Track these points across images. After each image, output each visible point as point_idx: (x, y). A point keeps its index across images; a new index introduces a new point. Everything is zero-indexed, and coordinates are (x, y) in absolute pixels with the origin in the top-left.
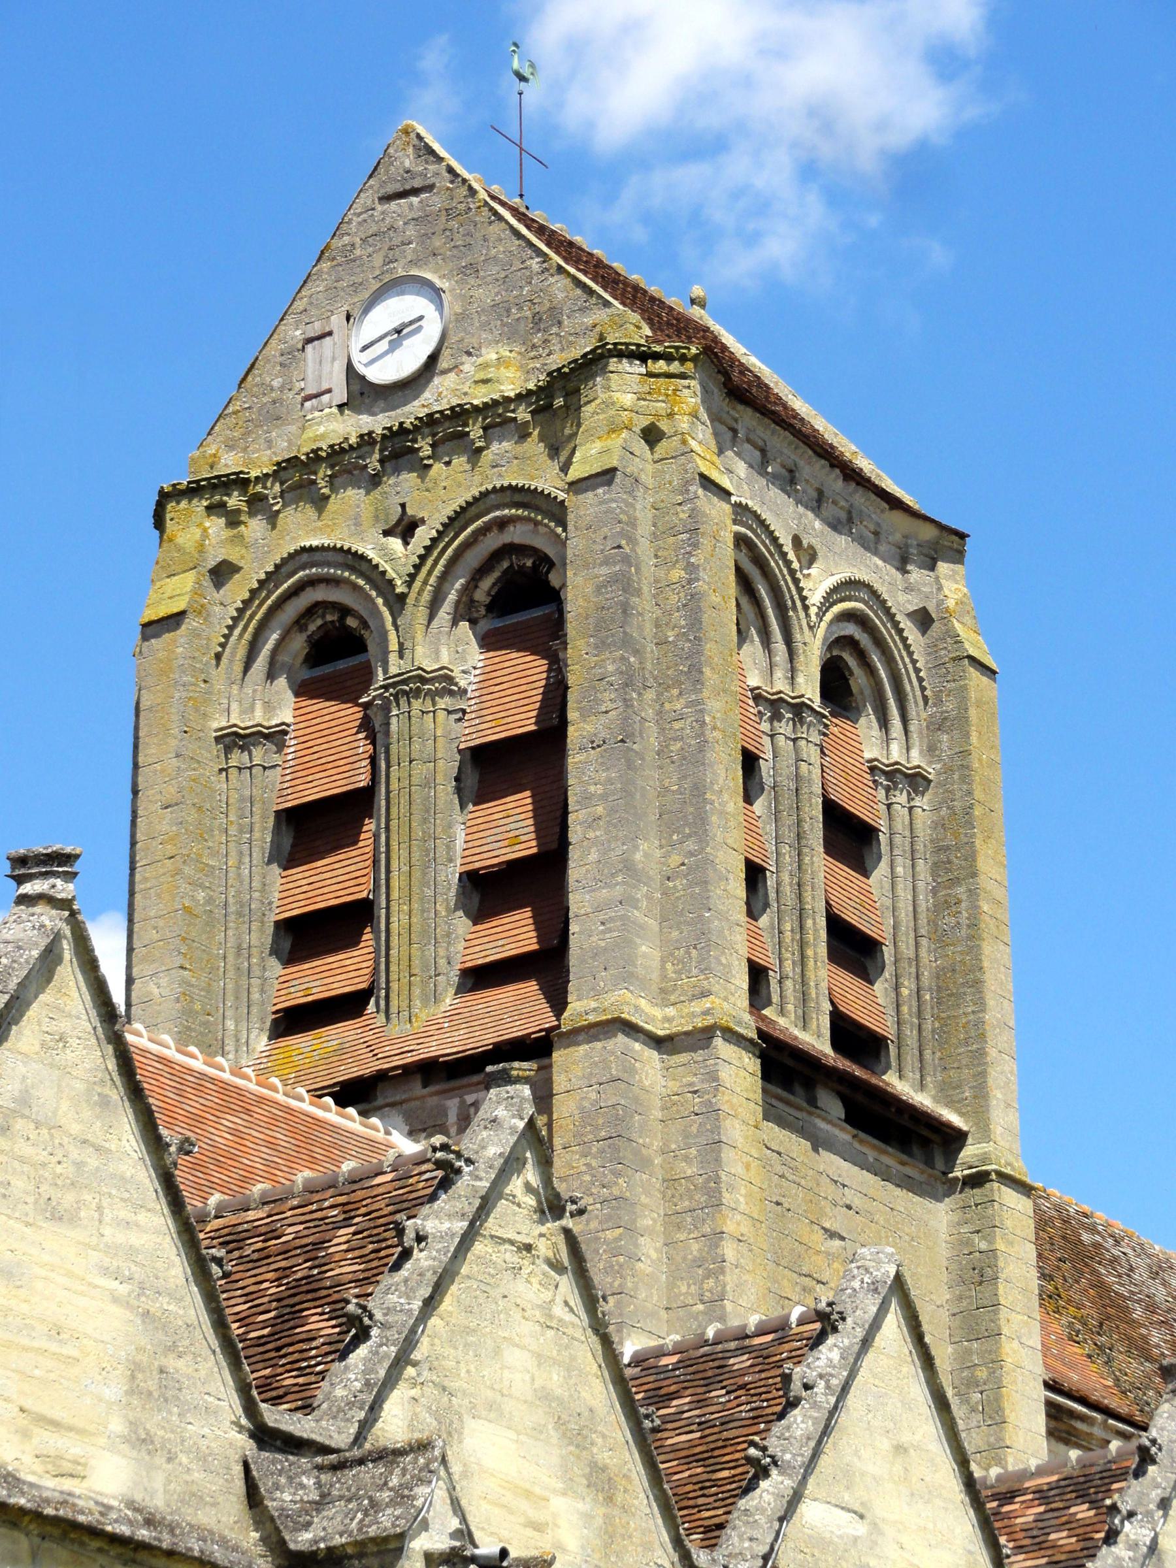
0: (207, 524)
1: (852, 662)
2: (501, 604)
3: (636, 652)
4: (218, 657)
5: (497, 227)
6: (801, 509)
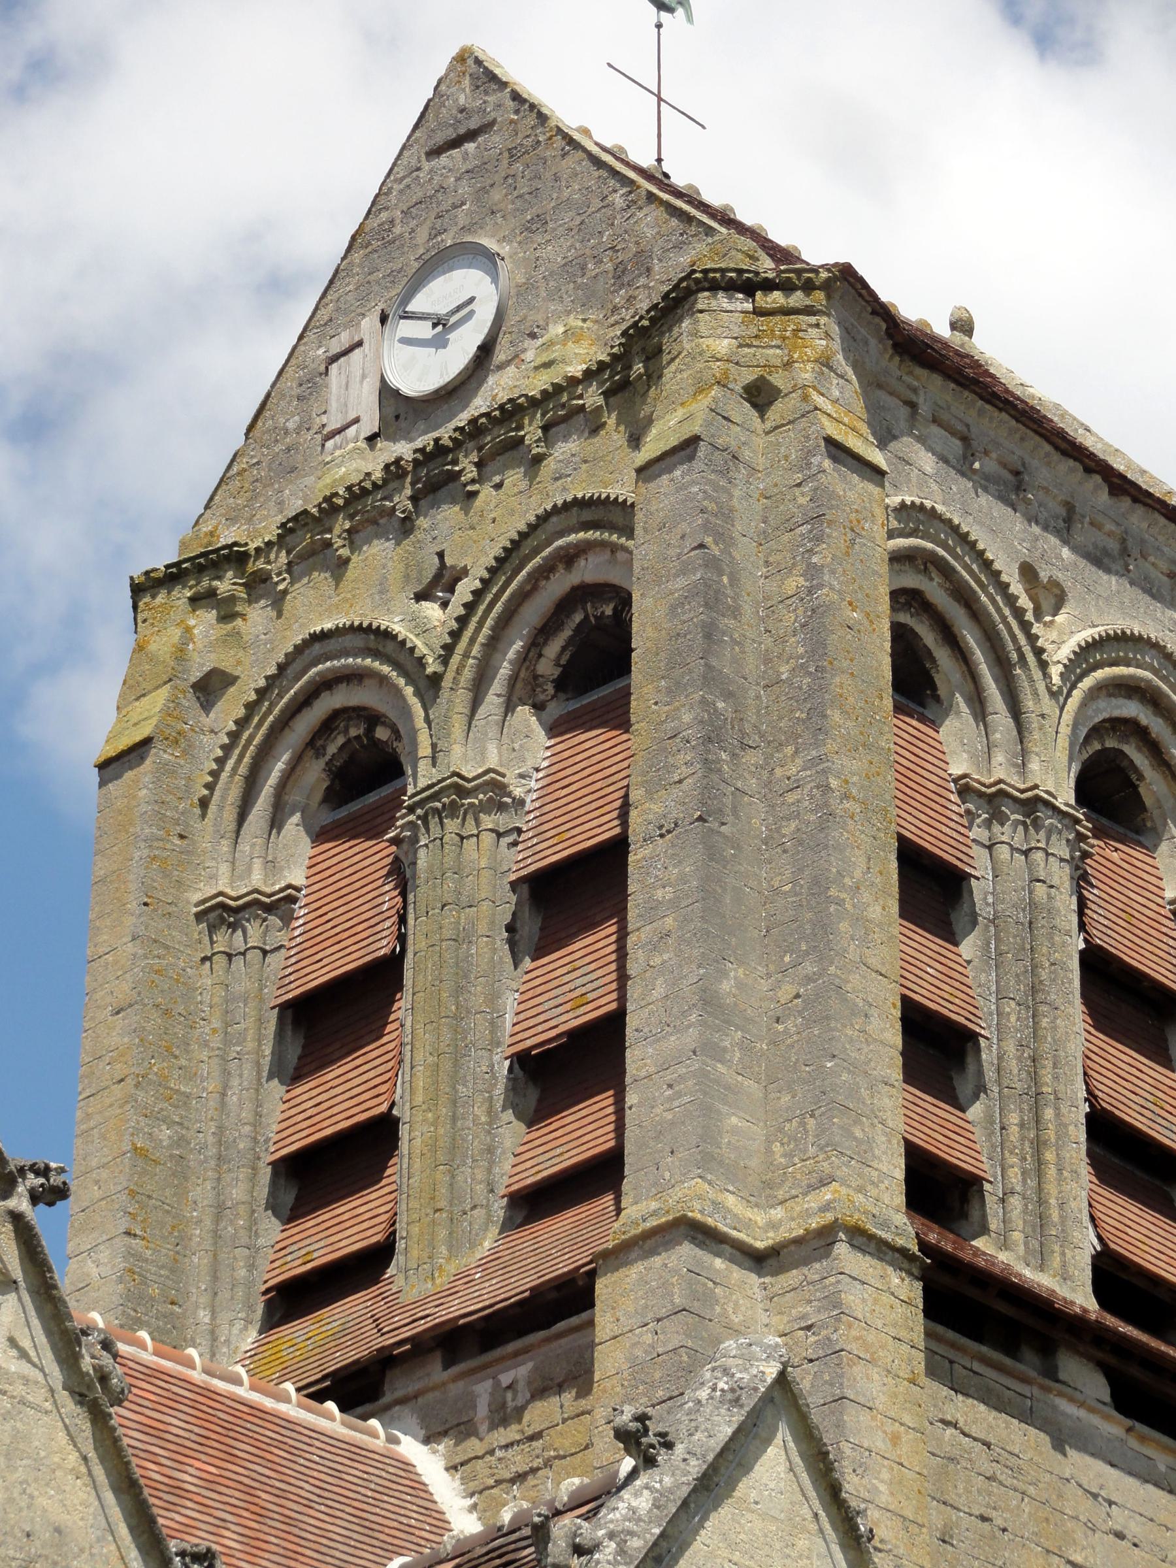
0: (192, 622)
1: (1140, 759)
3: (728, 695)
4: (204, 803)
6: (1036, 529)
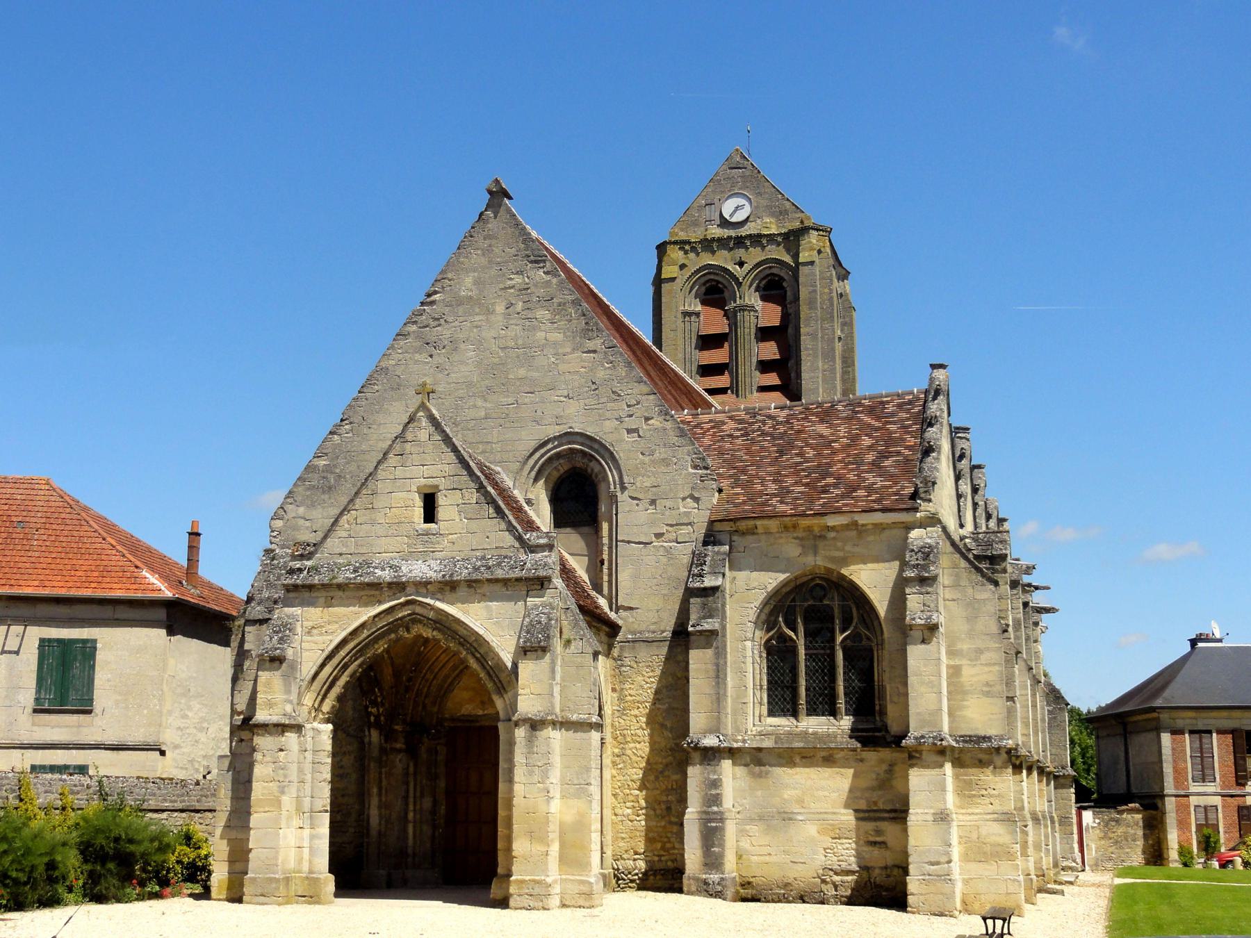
2: (766, 288)
5: (767, 184)
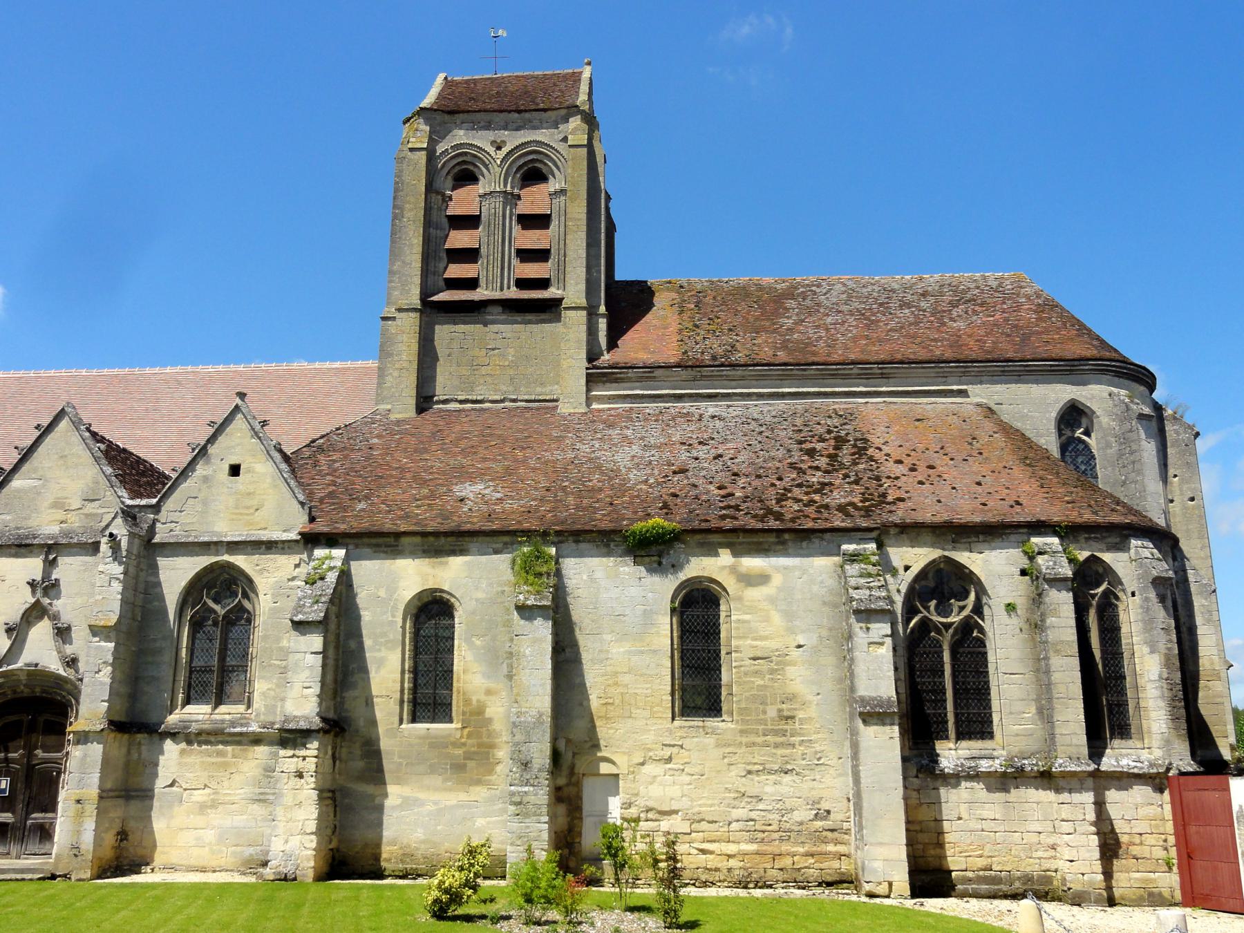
3: (398, 209)
